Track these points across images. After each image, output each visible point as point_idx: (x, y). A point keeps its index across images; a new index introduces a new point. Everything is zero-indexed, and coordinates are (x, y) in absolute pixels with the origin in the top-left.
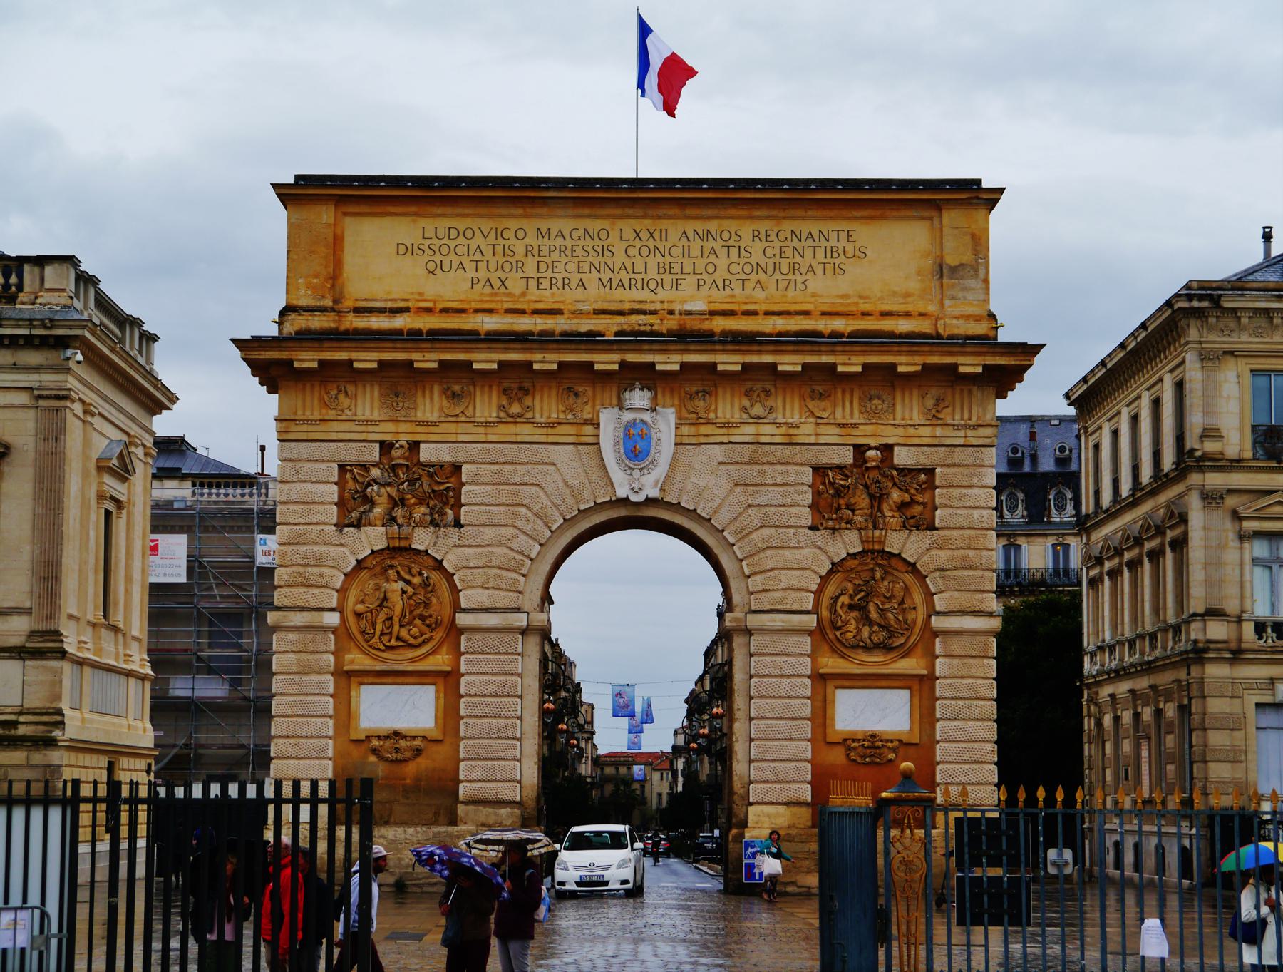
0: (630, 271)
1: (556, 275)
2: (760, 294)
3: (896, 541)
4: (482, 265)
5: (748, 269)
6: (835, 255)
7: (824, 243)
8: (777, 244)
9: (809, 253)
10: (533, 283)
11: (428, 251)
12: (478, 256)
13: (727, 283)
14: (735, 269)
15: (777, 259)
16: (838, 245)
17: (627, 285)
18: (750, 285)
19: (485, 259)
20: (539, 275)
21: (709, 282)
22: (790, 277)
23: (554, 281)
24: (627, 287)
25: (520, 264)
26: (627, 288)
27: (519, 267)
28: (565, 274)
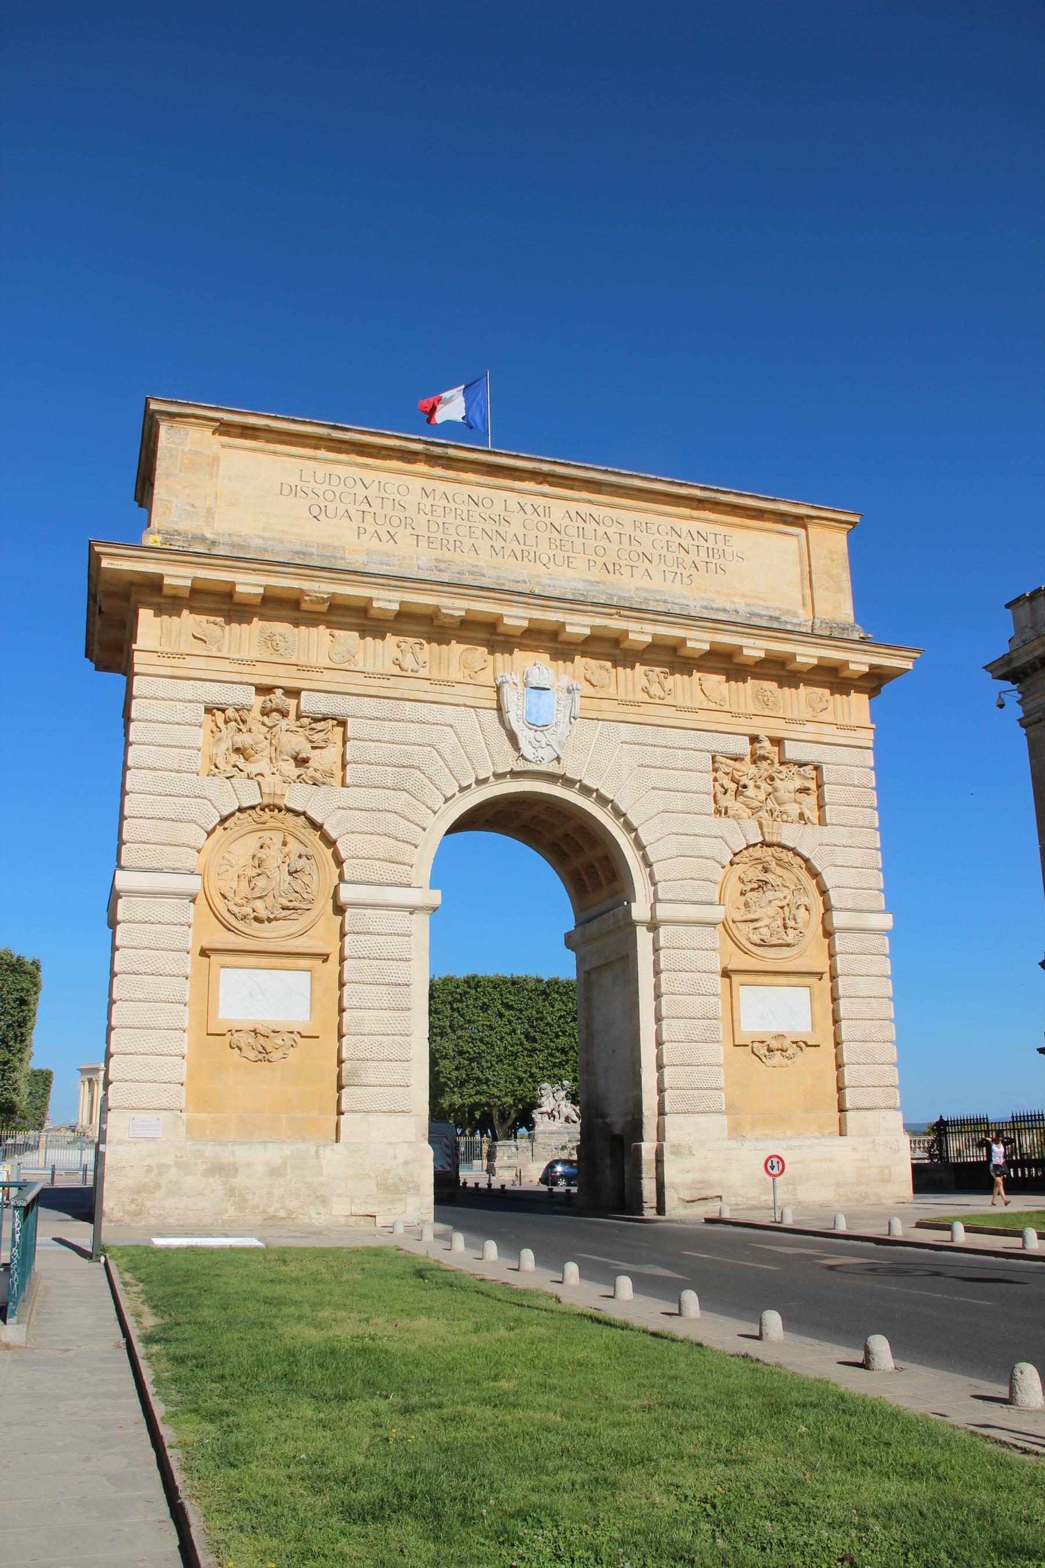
0: (522, 542)
1: (444, 536)
2: (645, 583)
3: (789, 834)
4: (369, 518)
5: (634, 556)
6: (716, 556)
7: (702, 542)
8: (665, 539)
9: (693, 551)
10: (423, 543)
11: (311, 494)
12: (365, 507)
13: (617, 567)
14: (624, 555)
15: (664, 552)
16: (715, 546)
17: (519, 556)
18: (639, 572)
19: (372, 510)
20: (430, 535)
21: (600, 565)
22: (675, 569)
23: (445, 542)
24: (519, 557)
25: (409, 521)
26: (519, 557)
27: (407, 522)
28: (457, 538)
